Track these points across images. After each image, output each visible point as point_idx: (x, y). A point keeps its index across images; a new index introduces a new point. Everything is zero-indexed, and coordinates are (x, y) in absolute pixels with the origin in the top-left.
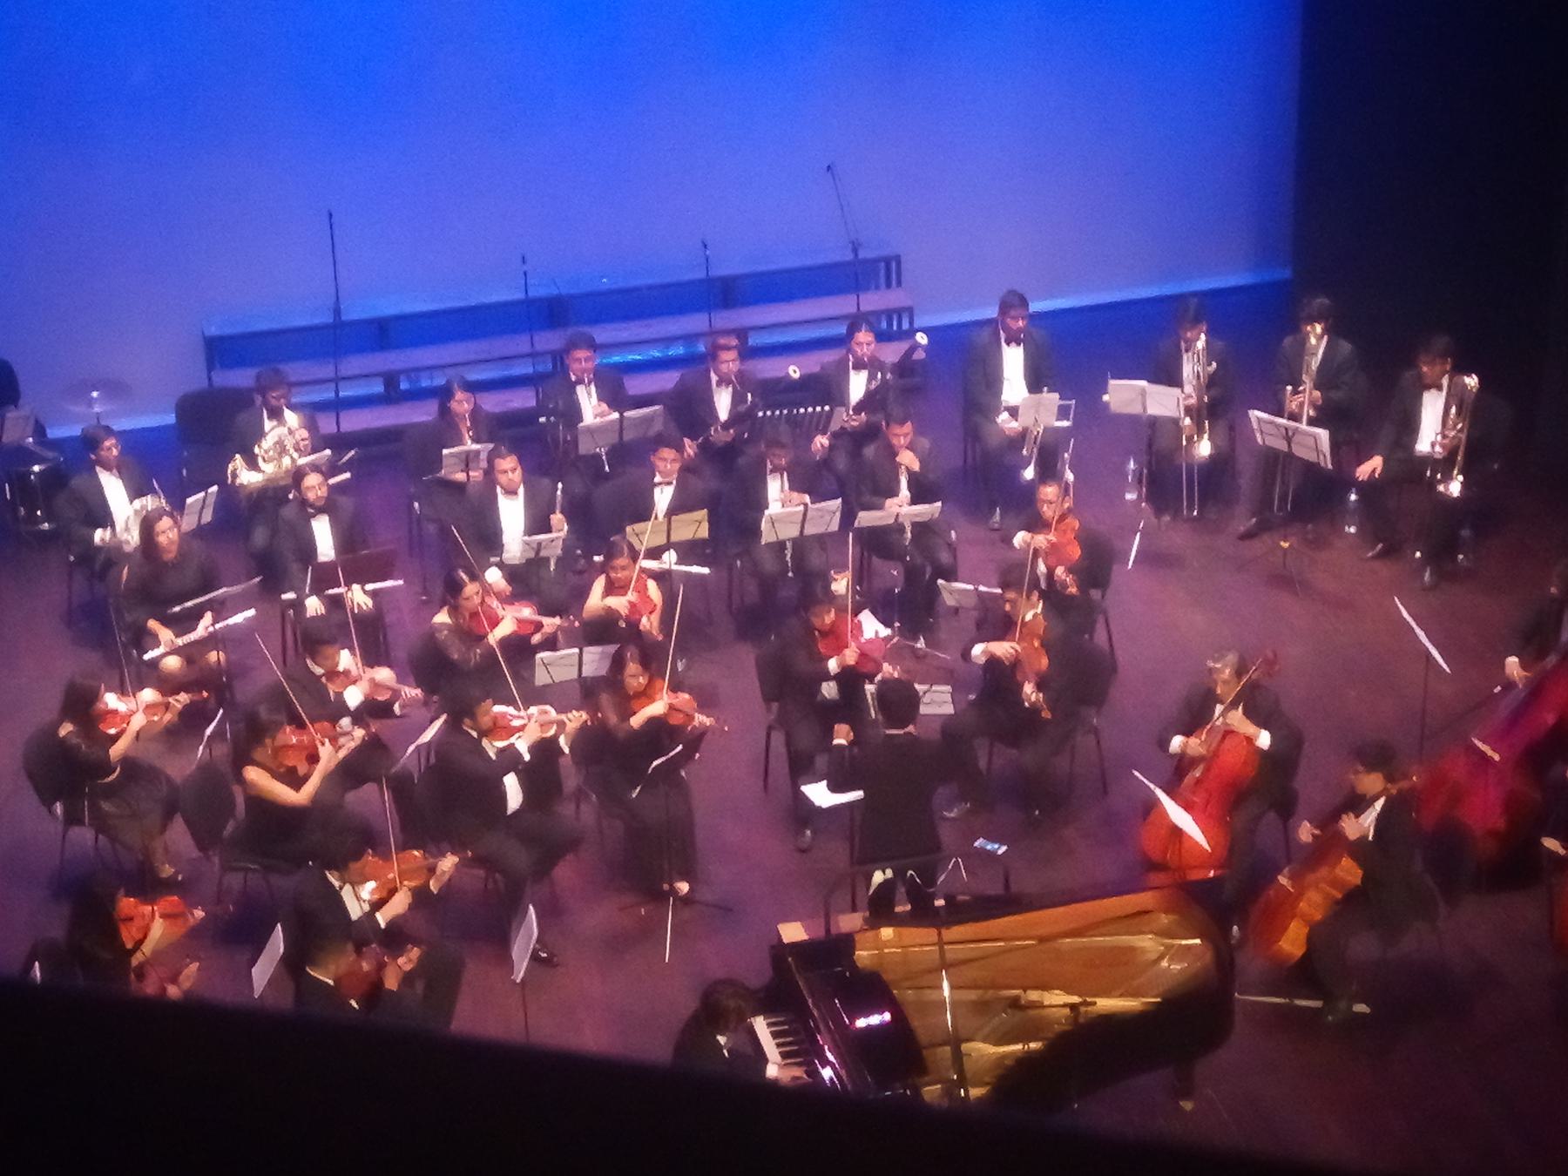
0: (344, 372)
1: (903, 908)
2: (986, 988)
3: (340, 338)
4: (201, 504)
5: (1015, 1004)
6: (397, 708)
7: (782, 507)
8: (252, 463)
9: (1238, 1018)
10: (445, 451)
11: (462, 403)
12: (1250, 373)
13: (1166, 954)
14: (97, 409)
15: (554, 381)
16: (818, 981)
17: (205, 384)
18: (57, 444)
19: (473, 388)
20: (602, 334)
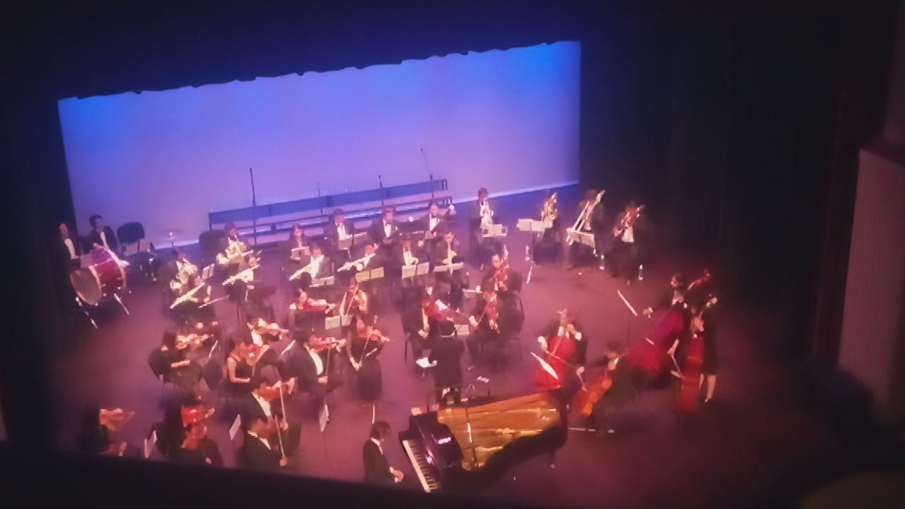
0: (257, 223)
1: (451, 402)
2: (484, 428)
3: (256, 212)
4: (208, 270)
5: (493, 434)
6: (281, 337)
7: (411, 265)
8: (225, 255)
9: (570, 436)
10: (293, 250)
11: (298, 233)
12: (567, 214)
13: (544, 415)
14: (172, 239)
15: (330, 225)
16: (423, 429)
17: (209, 229)
18: (158, 251)
19: (301, 227)
20: (346, 208)
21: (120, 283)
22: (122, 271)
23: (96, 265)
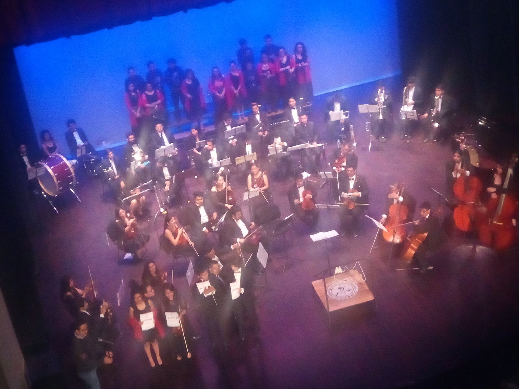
21: (71, 179)
22: (72, 170)
23: (52, 167)
